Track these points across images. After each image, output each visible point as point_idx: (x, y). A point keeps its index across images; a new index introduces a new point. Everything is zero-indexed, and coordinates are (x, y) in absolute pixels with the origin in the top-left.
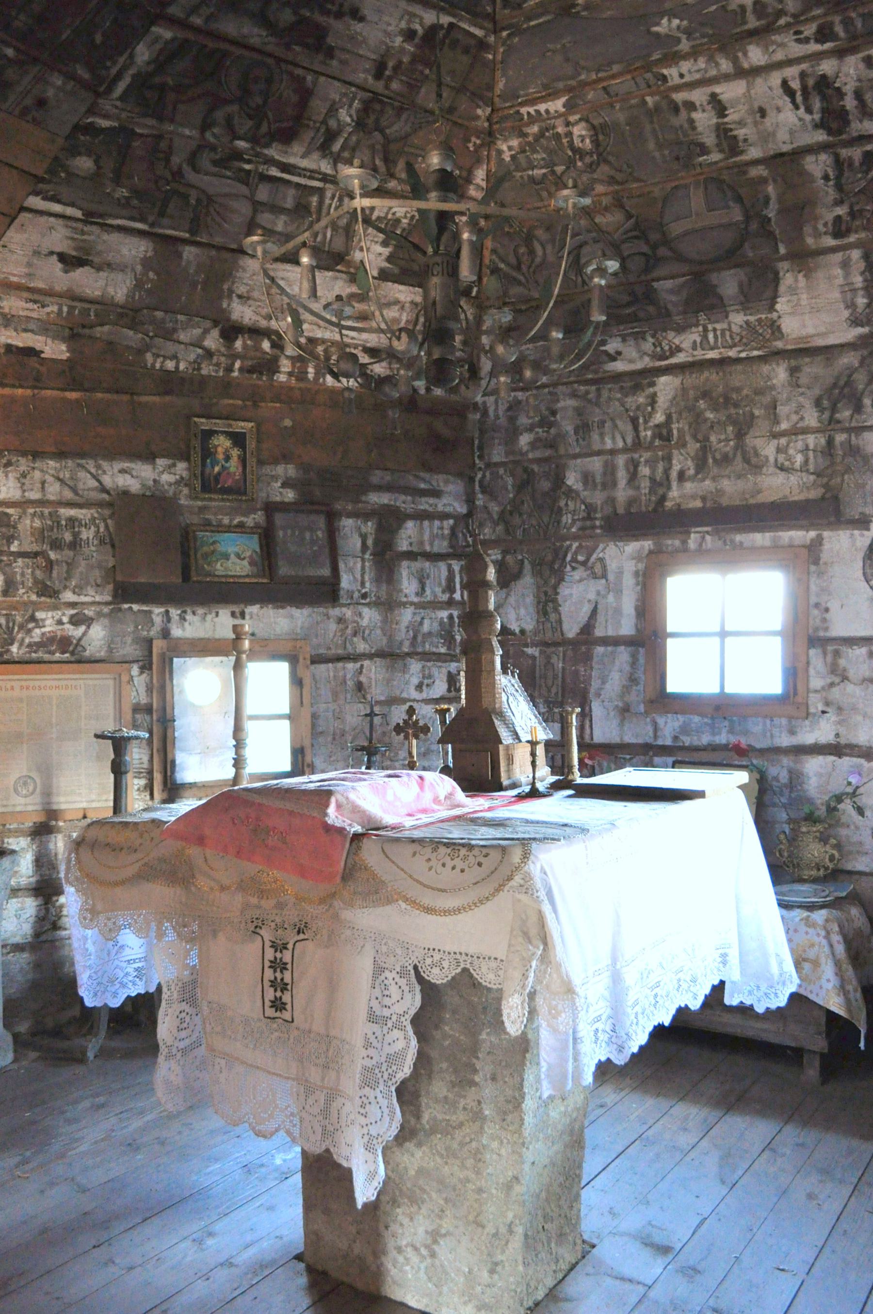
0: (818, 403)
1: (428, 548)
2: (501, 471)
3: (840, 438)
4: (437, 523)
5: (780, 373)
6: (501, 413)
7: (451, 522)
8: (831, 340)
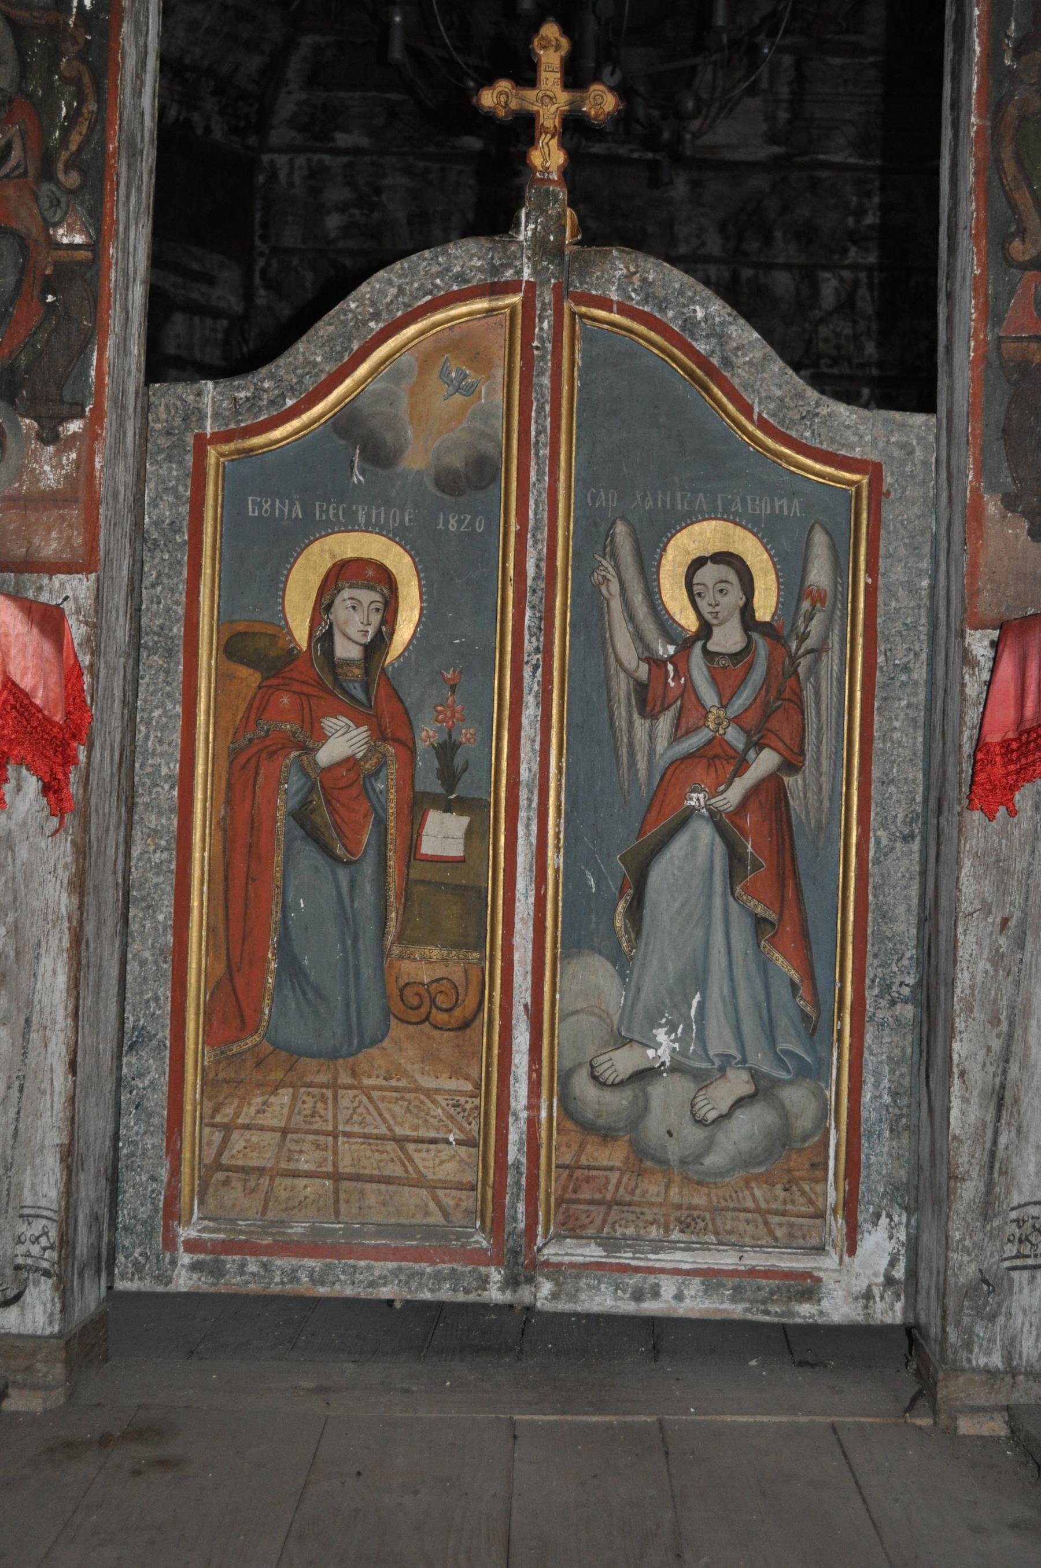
0: (722, 228)
1: (198, 355)
2: (295, 261)
3: (747, 273)
4: (209, 322)
5: (680, 188)
6: (297, 180)
7: (225, 323)
8: (741, 155)
